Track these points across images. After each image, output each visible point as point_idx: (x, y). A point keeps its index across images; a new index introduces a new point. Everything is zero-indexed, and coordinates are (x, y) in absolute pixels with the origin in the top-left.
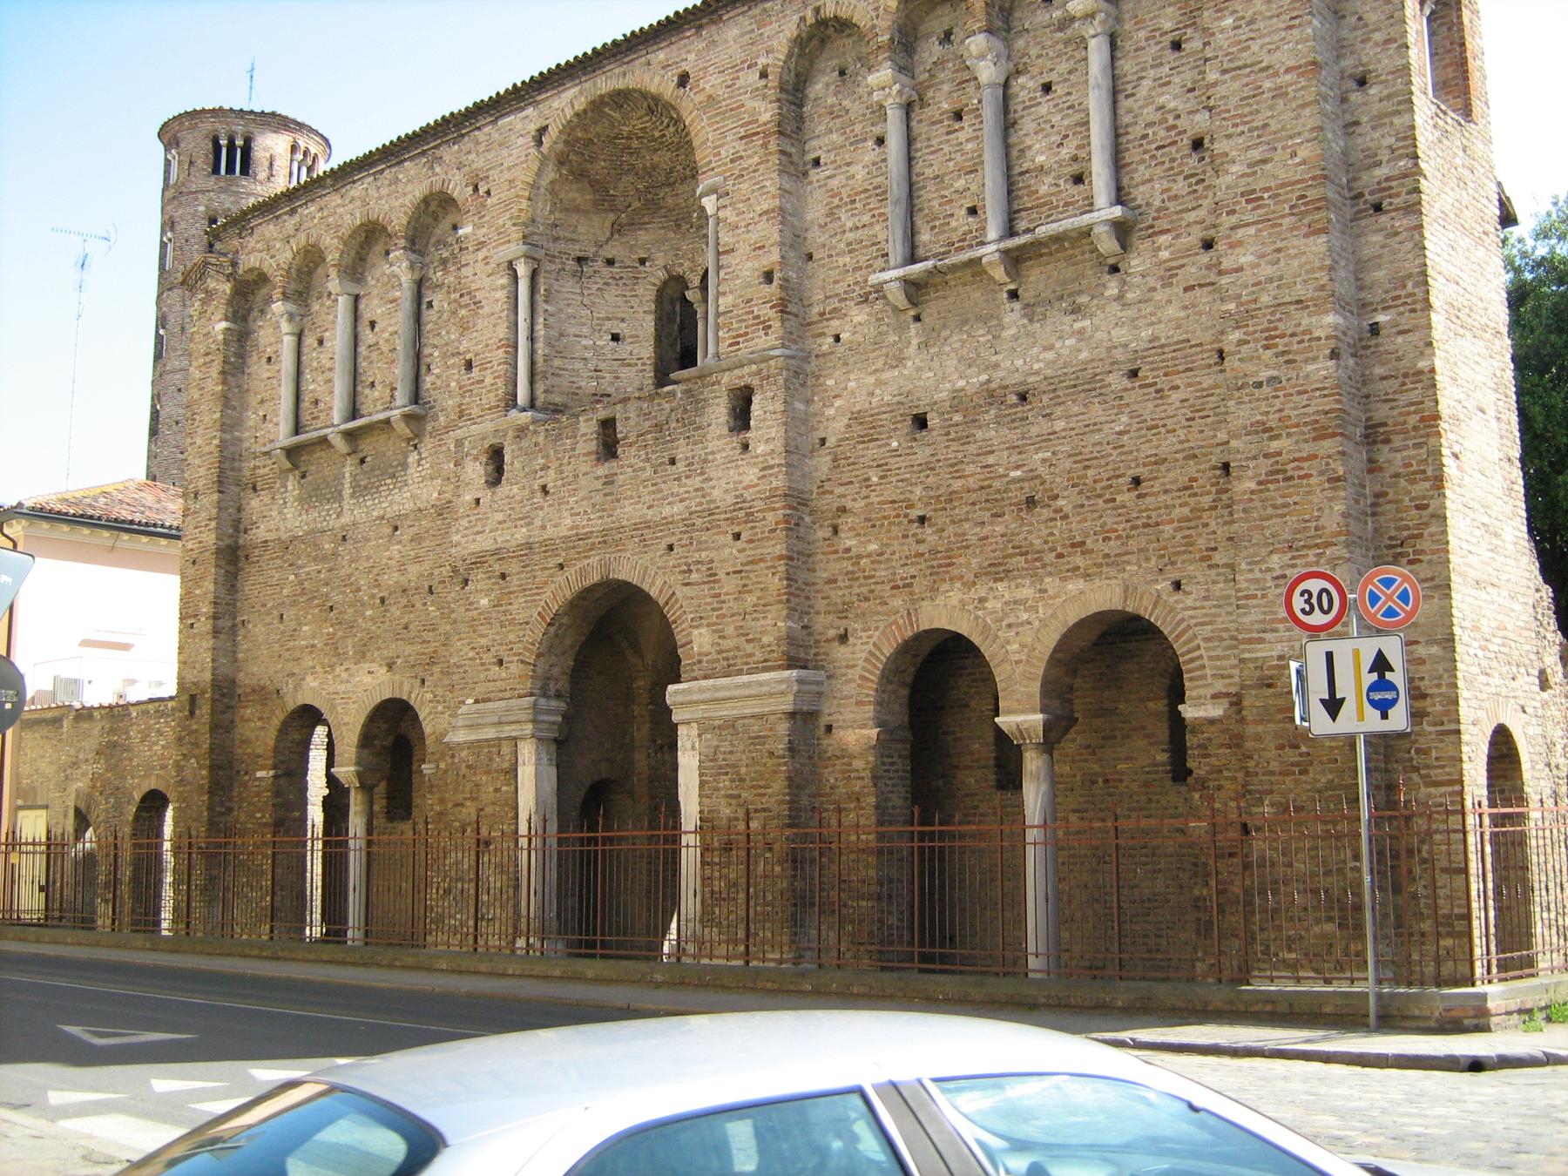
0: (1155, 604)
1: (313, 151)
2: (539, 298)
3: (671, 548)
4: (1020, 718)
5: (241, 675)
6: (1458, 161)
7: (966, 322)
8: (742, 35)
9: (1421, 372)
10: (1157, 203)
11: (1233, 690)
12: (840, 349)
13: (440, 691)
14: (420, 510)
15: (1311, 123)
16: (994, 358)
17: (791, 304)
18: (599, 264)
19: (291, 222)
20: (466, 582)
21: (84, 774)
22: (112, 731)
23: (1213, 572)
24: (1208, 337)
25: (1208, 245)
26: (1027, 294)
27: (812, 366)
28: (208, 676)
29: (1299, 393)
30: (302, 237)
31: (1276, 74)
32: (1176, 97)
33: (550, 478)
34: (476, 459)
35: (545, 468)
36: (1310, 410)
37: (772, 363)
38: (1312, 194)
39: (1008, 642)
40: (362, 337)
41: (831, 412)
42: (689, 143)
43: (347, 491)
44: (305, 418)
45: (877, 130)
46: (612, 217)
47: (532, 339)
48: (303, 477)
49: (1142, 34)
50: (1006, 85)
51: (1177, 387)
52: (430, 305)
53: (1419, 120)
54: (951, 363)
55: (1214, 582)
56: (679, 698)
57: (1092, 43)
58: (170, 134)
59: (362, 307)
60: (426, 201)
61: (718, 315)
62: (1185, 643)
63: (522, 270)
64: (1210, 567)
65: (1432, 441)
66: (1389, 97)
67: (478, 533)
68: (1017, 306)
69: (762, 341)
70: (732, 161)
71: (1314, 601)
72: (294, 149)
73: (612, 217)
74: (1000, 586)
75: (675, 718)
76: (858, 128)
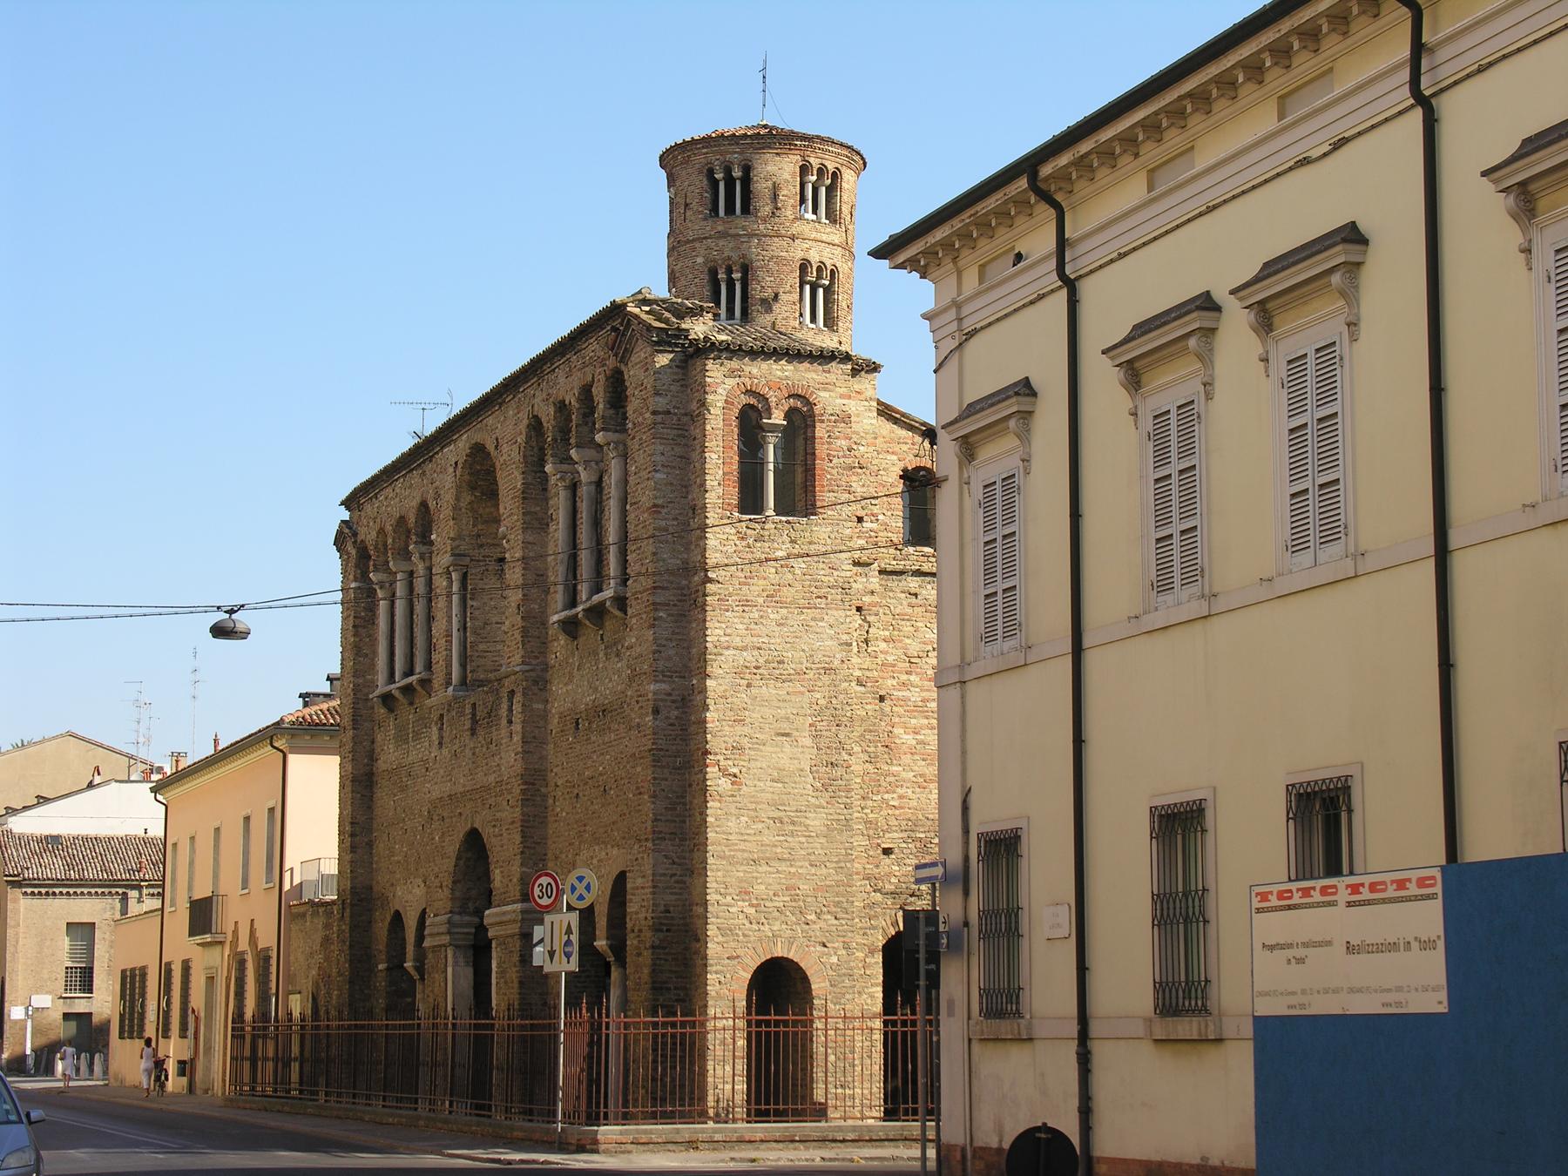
1: (831, 167)
58: (674, 159)
72: (804, 170)
75: (490, 934)
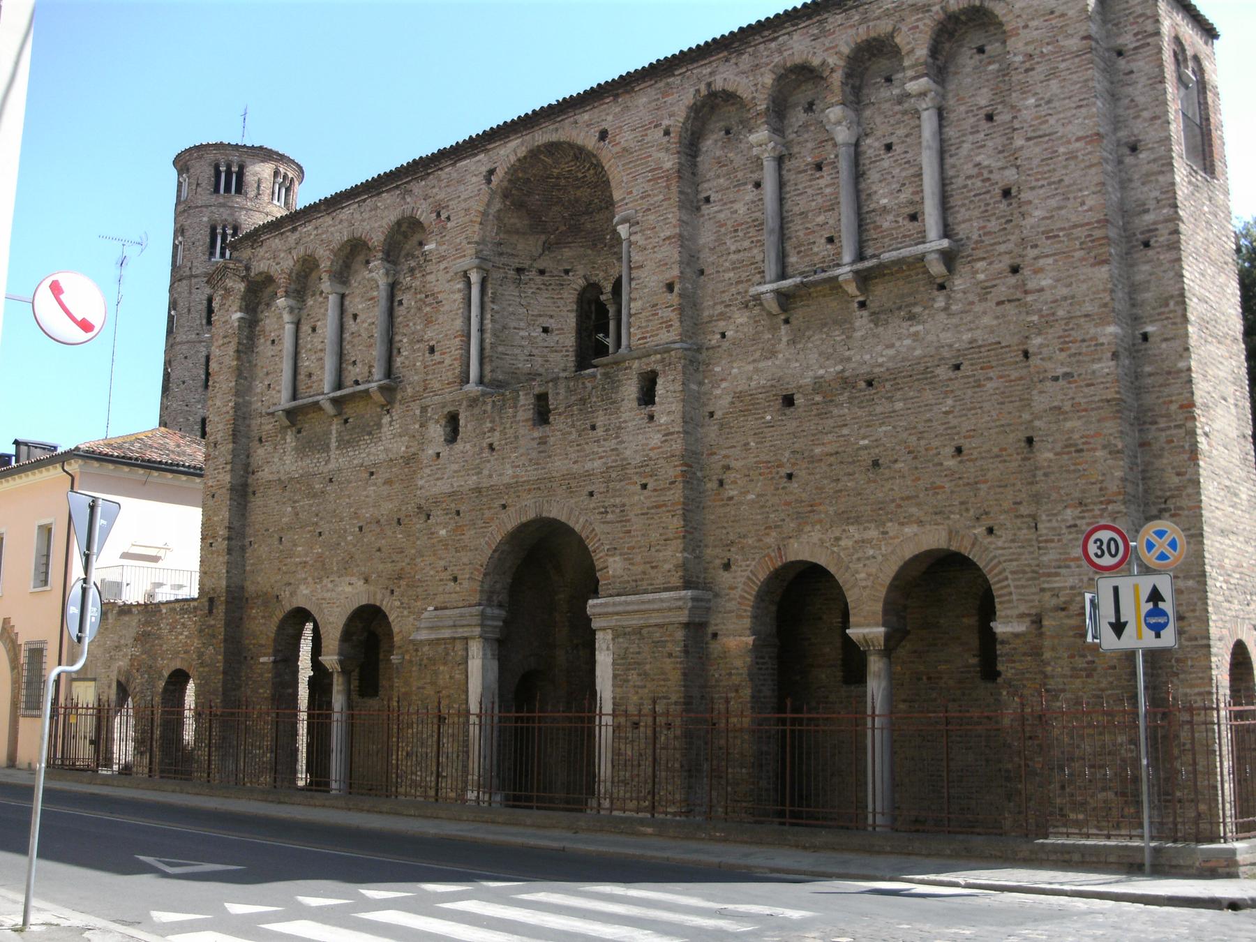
0: (973, 545)
1: (290, 176)
2: (486, 299)
3: (591, 494)
4: (866, 630)
5: (248, 584)
6: (1206, 209)
7: (825, 325)
8: (650, 103)
9: (1180, 371)
10: (975, 237)
11: (1033, 611)
12: (725, 344)
13: (405, 600)
14: (391, 460)
15: (1096, 180)
16: (847, 353)
17: (689, 307)
18: (533, 274)
19: (292, 238)
20: (428, 517)
21: (125, 655)
22: (147, 623)
23: (1019, 521)
24: (1015, 340)
25: (1015, 270)
26: (873, 305)
27: (703, 356)
28: (224, 583)
29: (1088, 385)
30: (302, 249)
31: (1069, 142)
32: (989, 157)
33: (495, 438)
34: (437, 422)
35: (492, 430)
36: (1096, 399)
37: (673, 353)
38: (1098, 233)
39: (857, 572)
40: (346, 326)
41: (718, 392)
42: (608, 182)
43: (334, 444)
44: (302, 387)
45: (755, 176)
46: (543, 237)
47: (482, 331)
48: (299, 432)
49: (963, 108)
50: (857, 145)
51: (991, 379)
52: (400, 303)
53: (1178, 179)
54: (813, 357)
55: (1020, 529)
56: (597, 610)
57: (925, 115)
58: (183, 162)
59: (347, 303)
60: (399, 223)
61: (630, 315)
62: (997, 575)
63: (475, 277)
64: (1017, 517)
65: (1189, 424)
66: (1155, 160)
67: (438, 479)
68: (865, 313)
69: (665, 337)
70: (642, 198)
71: (1105, 547)
72: (276, 174)
73: (543, 237)
74: (852, 529)
75: (594, 625)
76: (740, 175)
